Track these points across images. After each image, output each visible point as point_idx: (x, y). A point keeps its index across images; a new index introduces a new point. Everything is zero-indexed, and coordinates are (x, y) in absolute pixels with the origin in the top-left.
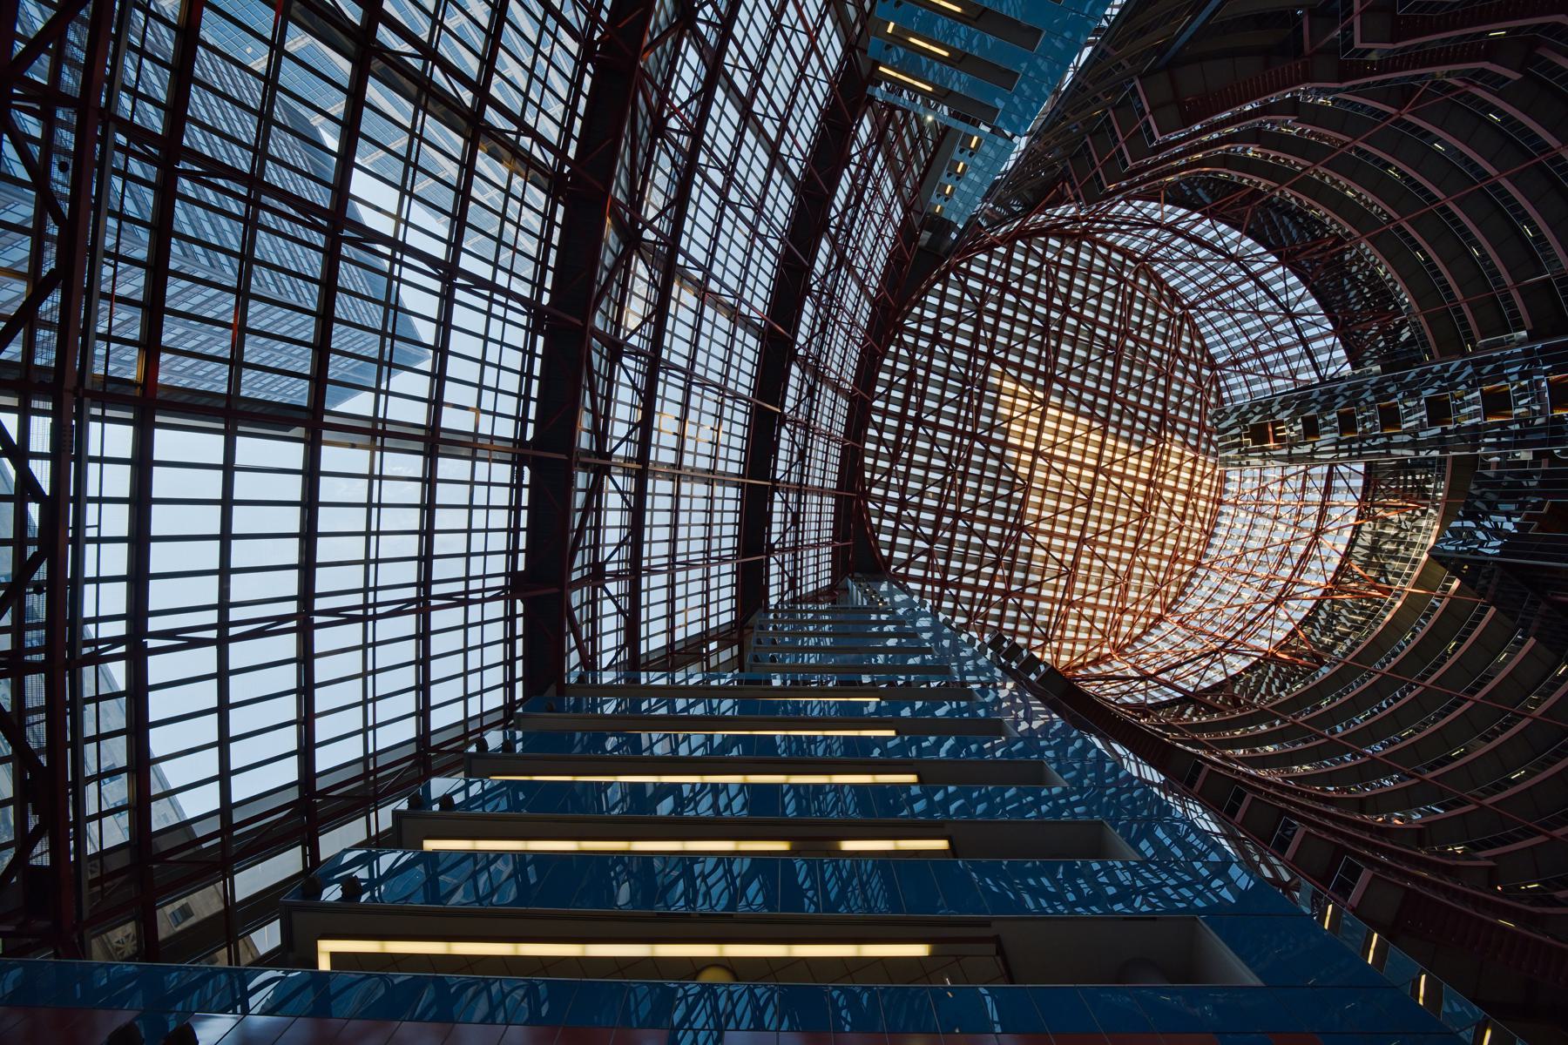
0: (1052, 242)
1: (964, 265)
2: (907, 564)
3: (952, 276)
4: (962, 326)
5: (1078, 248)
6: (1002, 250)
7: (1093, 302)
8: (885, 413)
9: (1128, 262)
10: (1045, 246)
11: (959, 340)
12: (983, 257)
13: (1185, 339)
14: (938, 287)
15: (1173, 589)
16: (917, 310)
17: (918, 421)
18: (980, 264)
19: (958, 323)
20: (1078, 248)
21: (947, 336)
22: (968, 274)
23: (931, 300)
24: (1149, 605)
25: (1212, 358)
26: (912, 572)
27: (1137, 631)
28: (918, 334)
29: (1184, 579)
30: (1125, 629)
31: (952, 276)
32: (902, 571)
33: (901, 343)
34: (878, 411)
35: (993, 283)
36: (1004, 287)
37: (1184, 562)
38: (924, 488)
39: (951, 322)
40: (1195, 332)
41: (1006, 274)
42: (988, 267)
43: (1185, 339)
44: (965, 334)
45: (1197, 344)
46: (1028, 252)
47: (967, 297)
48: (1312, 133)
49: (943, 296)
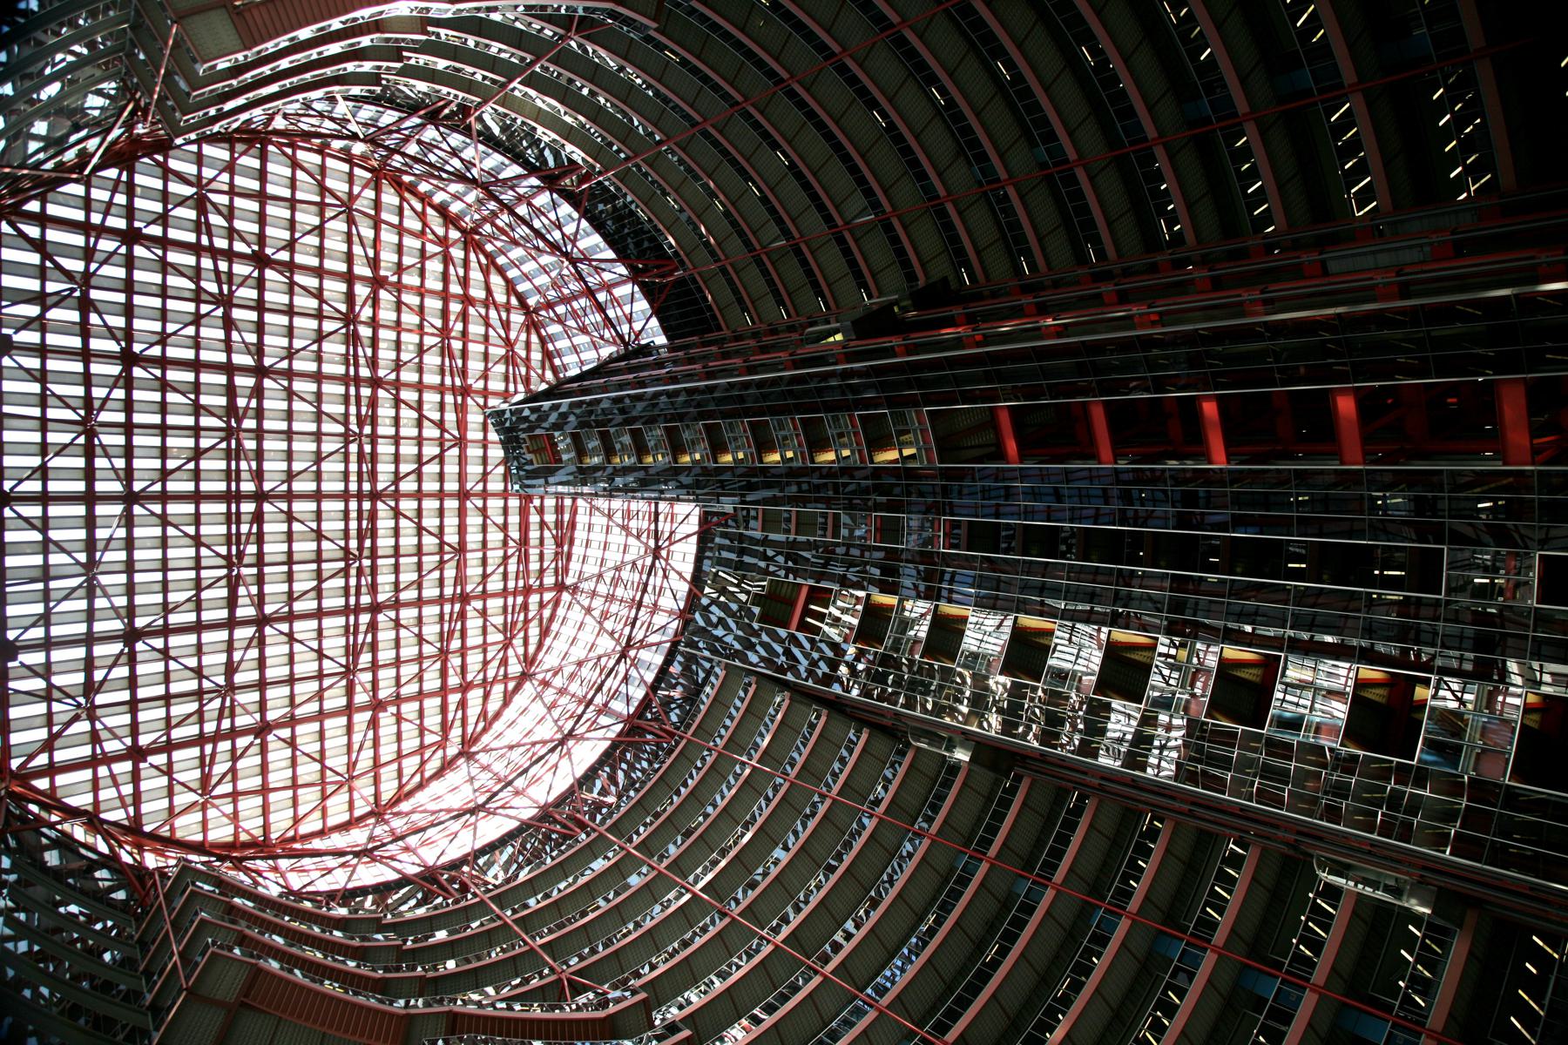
0: (208, 150)
1: (33, 206)
2: (48, 746)
4: (54, 314)
5: (263, 158)
7: (313, 240)
9: (357, 171)
10: (199, 160)
11: (53, 339)
12: (78, 189)
13: (476, 275)
15: (534, 631)
18: (68, 201)
19: (45, 309)
20: (263, 158)
21: (32, 337)
22: (43, 220)
24: (504, 662)
25: (522, 299)
26: (60, 756)
27: (493, 707)
29: (547, 613)
30: (473, 711)
32: (42, 759)
35: (102, 231)
36: (131, 237)
37: (542, 589)
38: (48, 611)
39: (33, 311)
40: (491, 265)
41: (130, 212)
42: (87, 204)
43: (476, 275)
44: (65, 327)
45: (496, 280)
46: (166, 173)
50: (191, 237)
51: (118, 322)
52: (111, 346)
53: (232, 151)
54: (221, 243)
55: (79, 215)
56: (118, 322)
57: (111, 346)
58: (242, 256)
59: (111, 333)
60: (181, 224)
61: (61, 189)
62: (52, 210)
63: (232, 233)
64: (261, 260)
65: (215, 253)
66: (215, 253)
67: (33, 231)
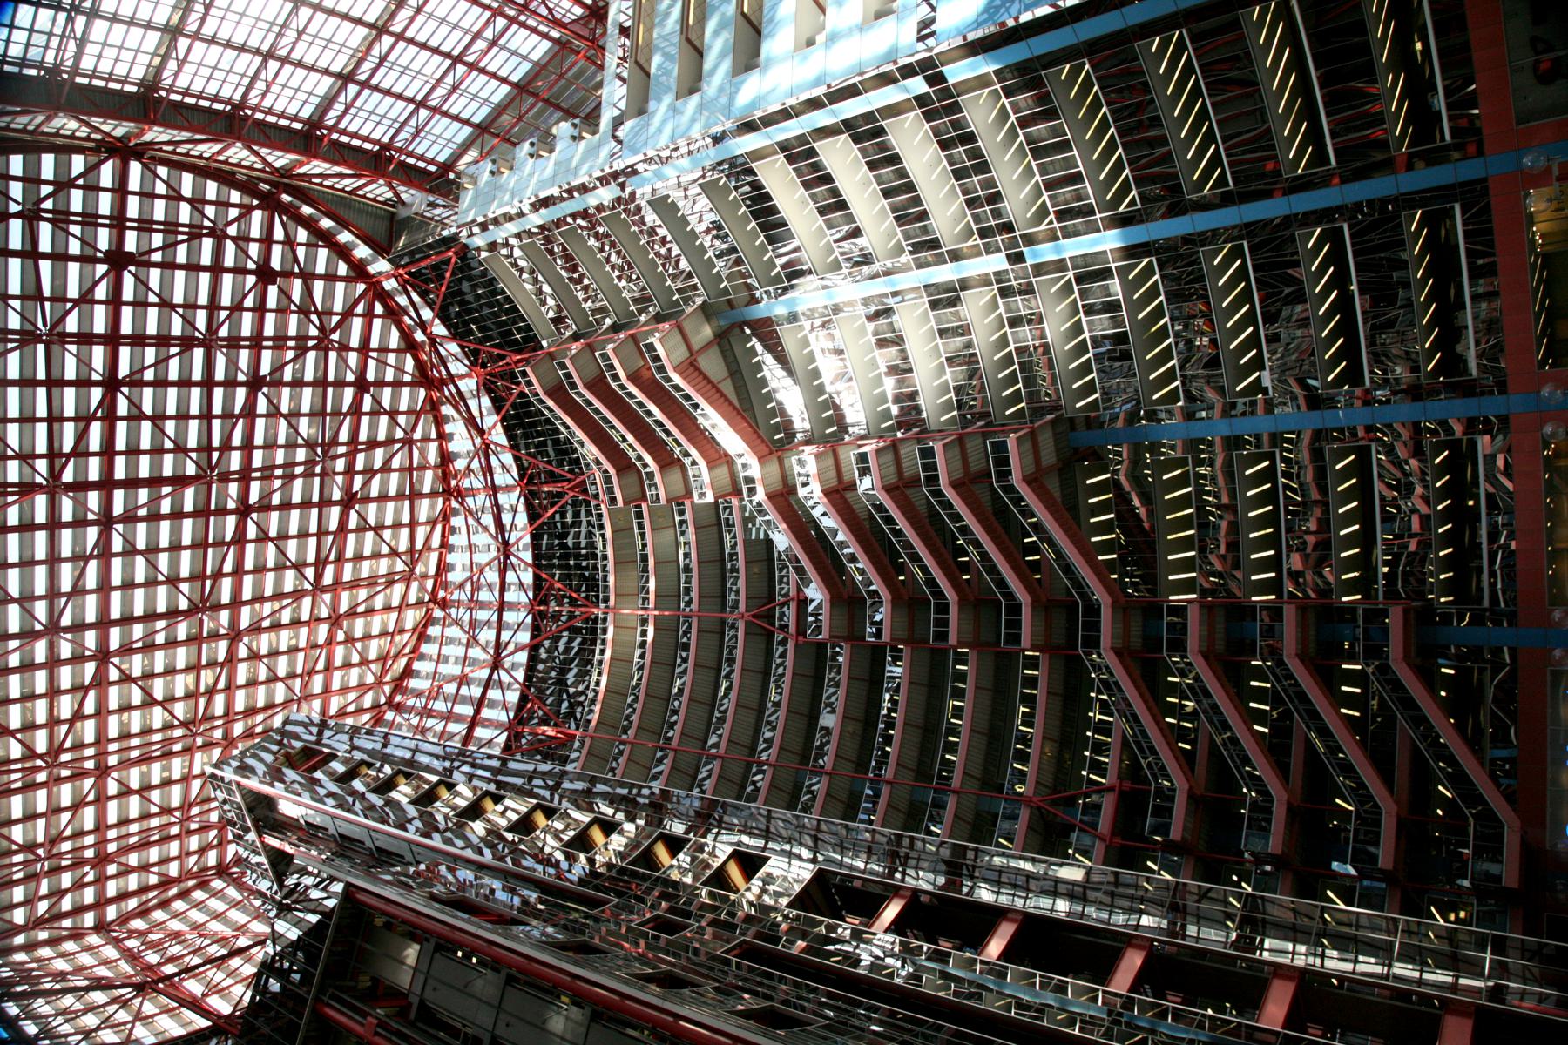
3: (361, 287)
6: (409, 364)
8: (120, 190)
12: (394, 339)
14: (342, 269)
16: (302, 235)
17: (118, 260)
18: (385, 335)
22: (369, 315)
23: (323, 253)
28: (267, 240)
31: (361, 287)
33: (247, 210)
34: (122, 176)
41: (380, 383)
42: (384, 350)
47: (335, 319)
48: (862, 572)
49: (331, 278)
50: (363, 437)
51: (288, 374)
52: (265, 369)
53: (436, 467)
54: (360, 460)
55: (374, 343)
56: (288, 374)
57: (265, 369)
58: (350, 483)
59: (278, 368)
60: (373, 427)
61: (393, 328)
62: (377, 323)
63: (369, 472)
64: (349, 501)
65: (351, 456)
66: (351, 456)
67: (360, 309)
